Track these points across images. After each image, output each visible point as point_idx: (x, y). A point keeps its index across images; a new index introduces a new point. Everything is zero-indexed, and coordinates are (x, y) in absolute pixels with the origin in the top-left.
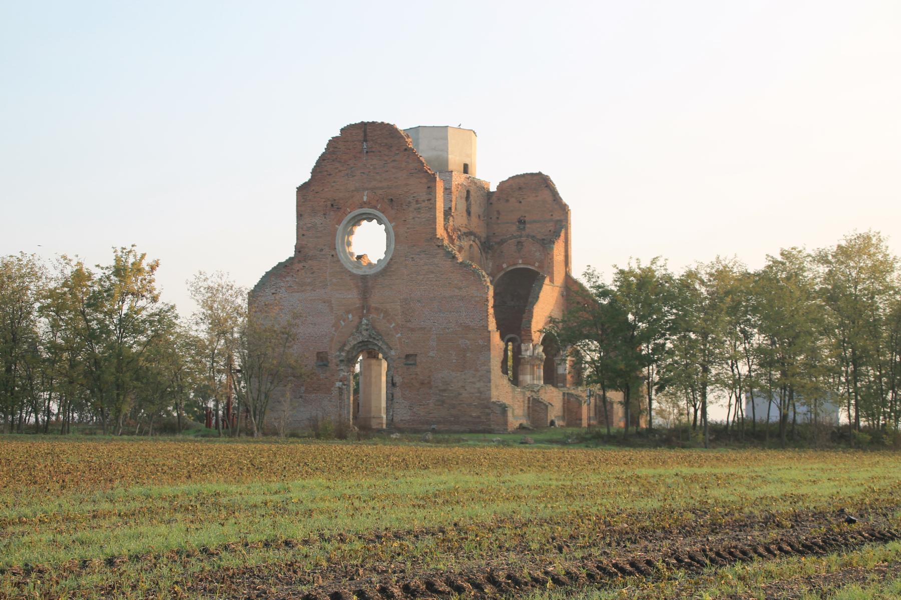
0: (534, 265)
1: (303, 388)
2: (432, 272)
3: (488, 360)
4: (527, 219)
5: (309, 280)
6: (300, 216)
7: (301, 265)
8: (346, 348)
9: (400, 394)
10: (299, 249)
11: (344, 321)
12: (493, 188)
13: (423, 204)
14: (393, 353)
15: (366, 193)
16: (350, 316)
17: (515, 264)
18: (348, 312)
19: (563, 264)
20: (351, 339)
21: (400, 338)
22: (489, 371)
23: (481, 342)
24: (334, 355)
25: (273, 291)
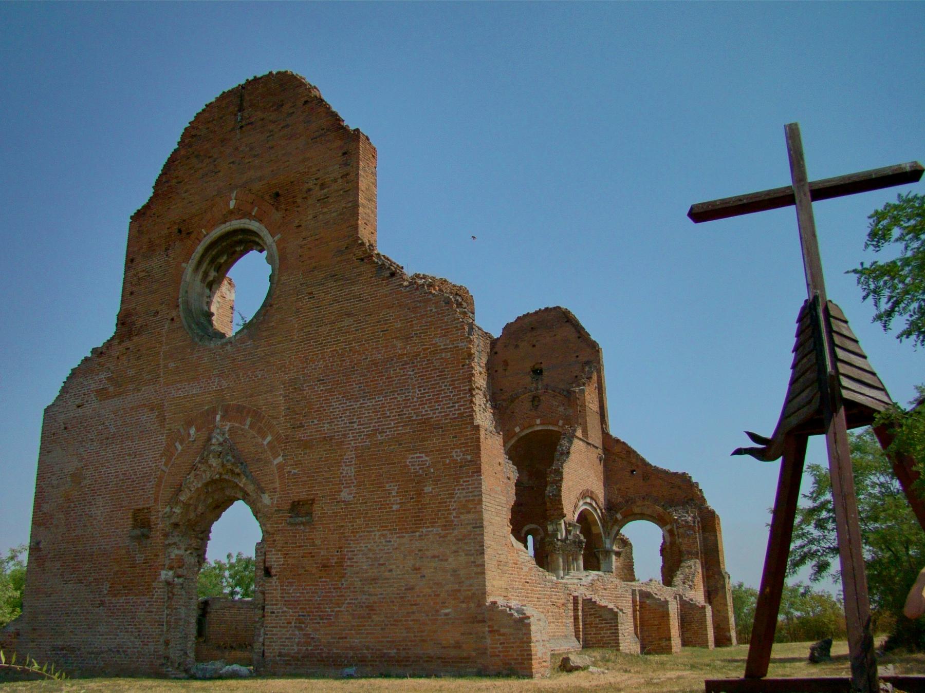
0: (556, 424)
1: (107, 585)
2: (349, 315)
3: (475, 503)
4: (543, 366)
5: (131, 372)
6: (130, 261)
7: (122, 348)
8: (182, 498)
9: (278, 594)
10: (124, 320)
11: (181, 444)
12: (497, 333)
13: (335, 186)
14: (266, 499)
15: (234, 195)
16: (192, 431)
17: (531, 426)
18: (189, 424)
19: (598, 417)
20: (191, 477)
21: (280, 467)
22: (479, 526)
23: (457, 455)
24: (163, 514)
25: (78, 402)
